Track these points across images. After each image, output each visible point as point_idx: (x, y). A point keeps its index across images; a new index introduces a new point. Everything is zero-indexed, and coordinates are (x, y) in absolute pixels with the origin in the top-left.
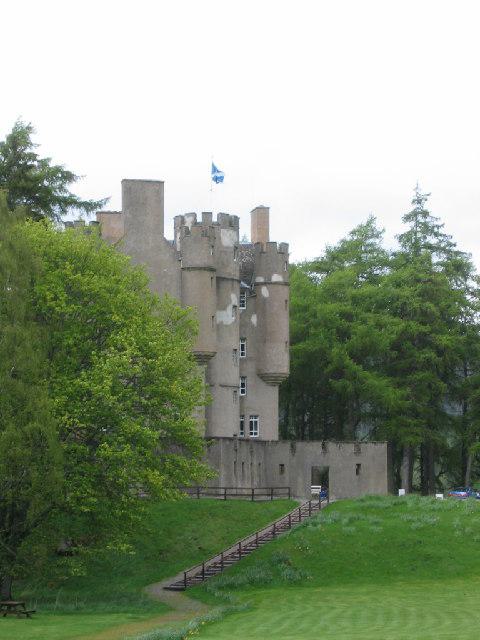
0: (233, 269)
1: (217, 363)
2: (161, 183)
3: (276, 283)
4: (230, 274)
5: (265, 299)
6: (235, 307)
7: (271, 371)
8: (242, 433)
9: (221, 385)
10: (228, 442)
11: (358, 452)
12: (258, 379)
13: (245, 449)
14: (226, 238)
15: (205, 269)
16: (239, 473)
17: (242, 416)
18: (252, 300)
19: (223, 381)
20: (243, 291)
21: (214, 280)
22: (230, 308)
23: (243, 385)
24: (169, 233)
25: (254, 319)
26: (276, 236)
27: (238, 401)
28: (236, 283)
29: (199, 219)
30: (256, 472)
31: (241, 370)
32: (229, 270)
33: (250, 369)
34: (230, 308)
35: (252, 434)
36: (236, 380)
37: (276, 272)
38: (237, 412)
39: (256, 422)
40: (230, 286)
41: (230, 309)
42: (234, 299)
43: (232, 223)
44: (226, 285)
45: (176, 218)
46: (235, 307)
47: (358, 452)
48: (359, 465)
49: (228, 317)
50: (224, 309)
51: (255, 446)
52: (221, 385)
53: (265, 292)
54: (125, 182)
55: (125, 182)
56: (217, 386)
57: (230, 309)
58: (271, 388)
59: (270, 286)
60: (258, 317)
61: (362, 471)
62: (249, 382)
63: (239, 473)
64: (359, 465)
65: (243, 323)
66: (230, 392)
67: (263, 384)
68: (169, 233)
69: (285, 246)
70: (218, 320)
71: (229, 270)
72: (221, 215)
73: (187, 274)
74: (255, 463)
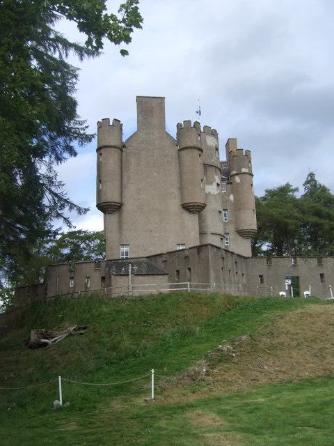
2: (162, 99)
3: (245, 173)
5: (238, 184)
6: (218, 185)
7: (245, 228)
9: (212, 234)
11: (320, 263)
12: (237, 235)
15: (194, 148)
18: (229, 185)
19: (213, 231)
25: (232, 197)
33: (231, 228)
43: (214, 133)
44: (211, 171)
47: (320, 263)
48: (322, 275)
51: (239, 260)
52: (212, 234)
53: (237, 179)
54: (140, 100)
55: (140, 100)
57: (215, 185)
58: (245, 241)
59: (241, 175)
60: (234, 196)
61: (326, 279)
64: (322, 275)
65: (224, 198)
73: (182, 152)
74: (239, 273)
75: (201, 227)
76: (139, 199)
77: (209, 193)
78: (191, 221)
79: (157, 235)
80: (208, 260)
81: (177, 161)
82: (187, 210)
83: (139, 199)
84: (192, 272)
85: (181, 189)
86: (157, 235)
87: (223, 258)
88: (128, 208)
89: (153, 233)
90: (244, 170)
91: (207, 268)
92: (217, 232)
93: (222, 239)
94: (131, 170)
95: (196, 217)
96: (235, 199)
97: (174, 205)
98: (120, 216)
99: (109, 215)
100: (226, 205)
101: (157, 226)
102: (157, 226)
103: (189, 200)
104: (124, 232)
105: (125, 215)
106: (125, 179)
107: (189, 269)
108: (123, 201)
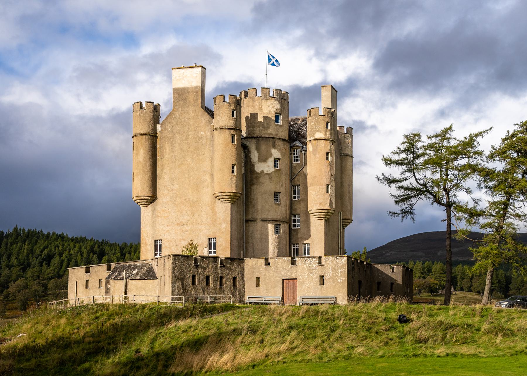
4: (271, 134)
9: (263, 220)
19: (264, 216)
32: (269, 131)
40: (271, 143)
48: (322, 277)
52: (263, 220)
56: (259, 220)
57: (271, 162)
64: (322, 277)
71: (269, 131)
77: (262, 172)
79: (188, 228)
83: (172, 190)
86: (188, 228)
89: (185, 226)
92: (270, 217)
94: (165, 158)
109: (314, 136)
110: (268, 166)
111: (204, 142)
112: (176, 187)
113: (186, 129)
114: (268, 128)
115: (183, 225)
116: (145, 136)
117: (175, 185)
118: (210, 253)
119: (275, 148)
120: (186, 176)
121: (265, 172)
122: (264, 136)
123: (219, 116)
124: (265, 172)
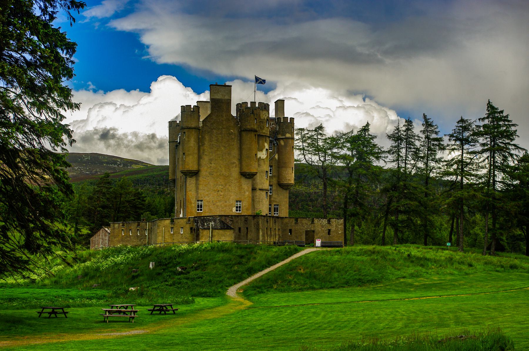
0: (266, 130)
1: (258, 177)
4: (264, 133)
6: (267, 150)
8: (270, 214)
9: (260, 190)
10: (263, 218)
13: (272, 221)
14: (263, 116)
16: (269, 233)
17: (270, 205)
20: (271, 142)
21: (257, 136)
22: (265, 150)
23: (271, 189)
24: (234, 113)
25: (276, 157)
26: (288, 113)
27: (268, 198)
28: (268, 139)
29: (249, 105)
30: (277, 233)
31: (270, 182)
32: (264, 131)
33: (275, 181)
34: (265, 150)
35: (275, 214)
36: (266, 186)
37: (289, 133)
38: (268, 203)
39: (277, 208)
40: (264, 139)
41: (264, 152)
42: (267, 146)
45: (238, 105)
46: (267, 150)
48: (329, 230)
49: (263, 155)
50: (262, 150)
51: (277, 220)
52: (260, 190)
56: (257, 189)
57: (264, 152)
58: (284, 191)
59: (285, 140)
60: (278, 156)
61: (331, 233)
62: (274, 188)
63: (269, 233)
64: (329, 230)
65: (271, 159)
66: (264, 193)
67: (281, 189)
68: (234, 113)
69: (292, 119)
70: (258, 156)
71: (264, 131)
72: (260, 103)
74: (277, 229)
75: (253, 185)
76: (211, 167)
77: (260, 157)
78: (246, 185)
79: (222, 194)
80: (259, 225)
81: (239, 138)
82: (244, 176)
84: (249, 230)
85: (240, 160)
86: (222, 194)
87: (267, 222)
88: (204, 172)
89: (220, 192)
90: (288, 135)
91: (258, 229)
93: (267, 193)
95: (250, 181)
96: (279, 158)
97: (235, 172)
98: (197, 180)
99: (191, 178)
100: (272, 163)
101: (222, 187)
102: (222, 187)
103: (246, 170)
104: (200, 191)
105: (201, 179)
106: (201, 151)
107: (247, 228)
108: (200, 168)
109: (285, 135)
110: (263, 154)
111: (233, 137)
112: (213, 165)
113: (221, 127)
114: (263, 129)
115: (218, 191)
116: (194, 130)
117: (213, 164)
118: (237, 210)
119: (266, 143)
120: (221, 158)
121: (262, 158)
122: (261, 134)
123: (247, 121)
124: (262, 158)
